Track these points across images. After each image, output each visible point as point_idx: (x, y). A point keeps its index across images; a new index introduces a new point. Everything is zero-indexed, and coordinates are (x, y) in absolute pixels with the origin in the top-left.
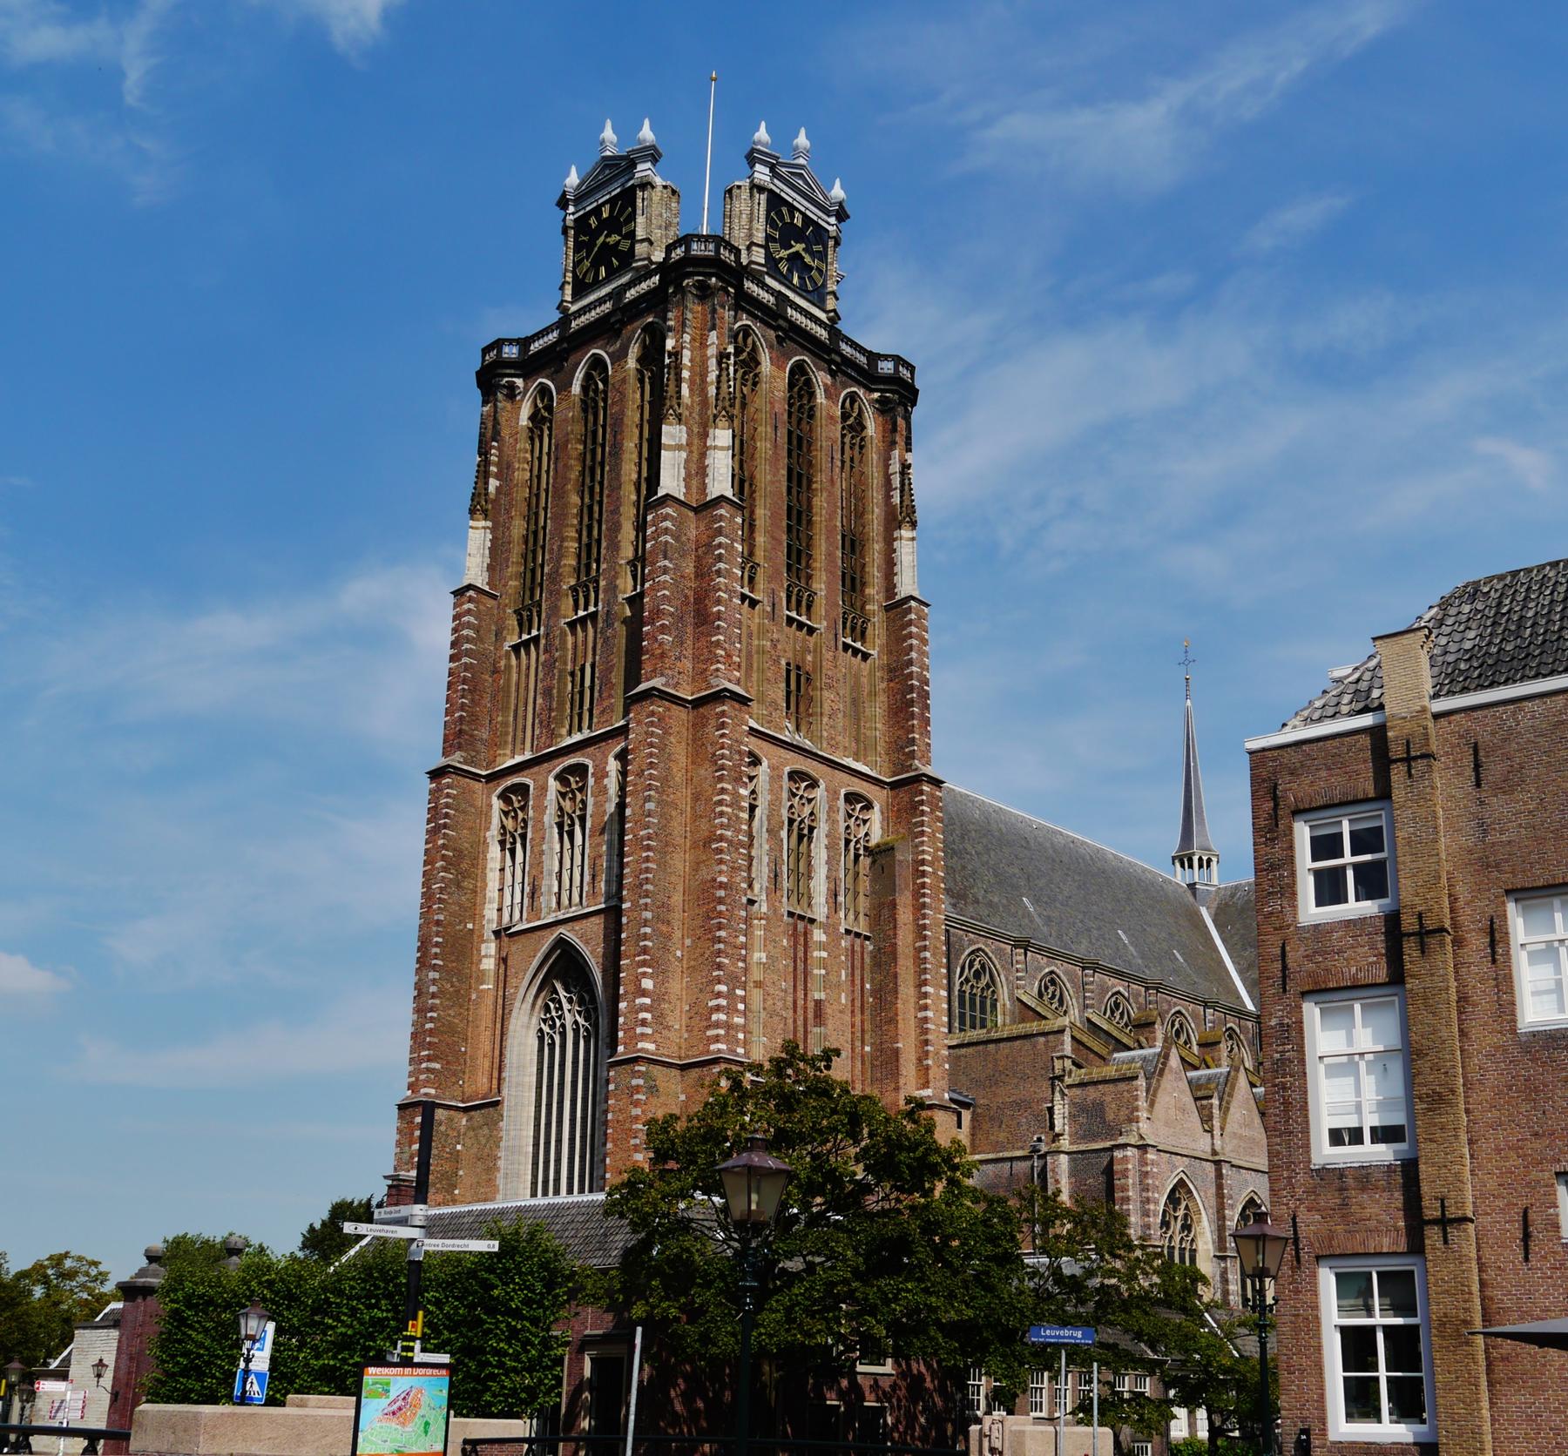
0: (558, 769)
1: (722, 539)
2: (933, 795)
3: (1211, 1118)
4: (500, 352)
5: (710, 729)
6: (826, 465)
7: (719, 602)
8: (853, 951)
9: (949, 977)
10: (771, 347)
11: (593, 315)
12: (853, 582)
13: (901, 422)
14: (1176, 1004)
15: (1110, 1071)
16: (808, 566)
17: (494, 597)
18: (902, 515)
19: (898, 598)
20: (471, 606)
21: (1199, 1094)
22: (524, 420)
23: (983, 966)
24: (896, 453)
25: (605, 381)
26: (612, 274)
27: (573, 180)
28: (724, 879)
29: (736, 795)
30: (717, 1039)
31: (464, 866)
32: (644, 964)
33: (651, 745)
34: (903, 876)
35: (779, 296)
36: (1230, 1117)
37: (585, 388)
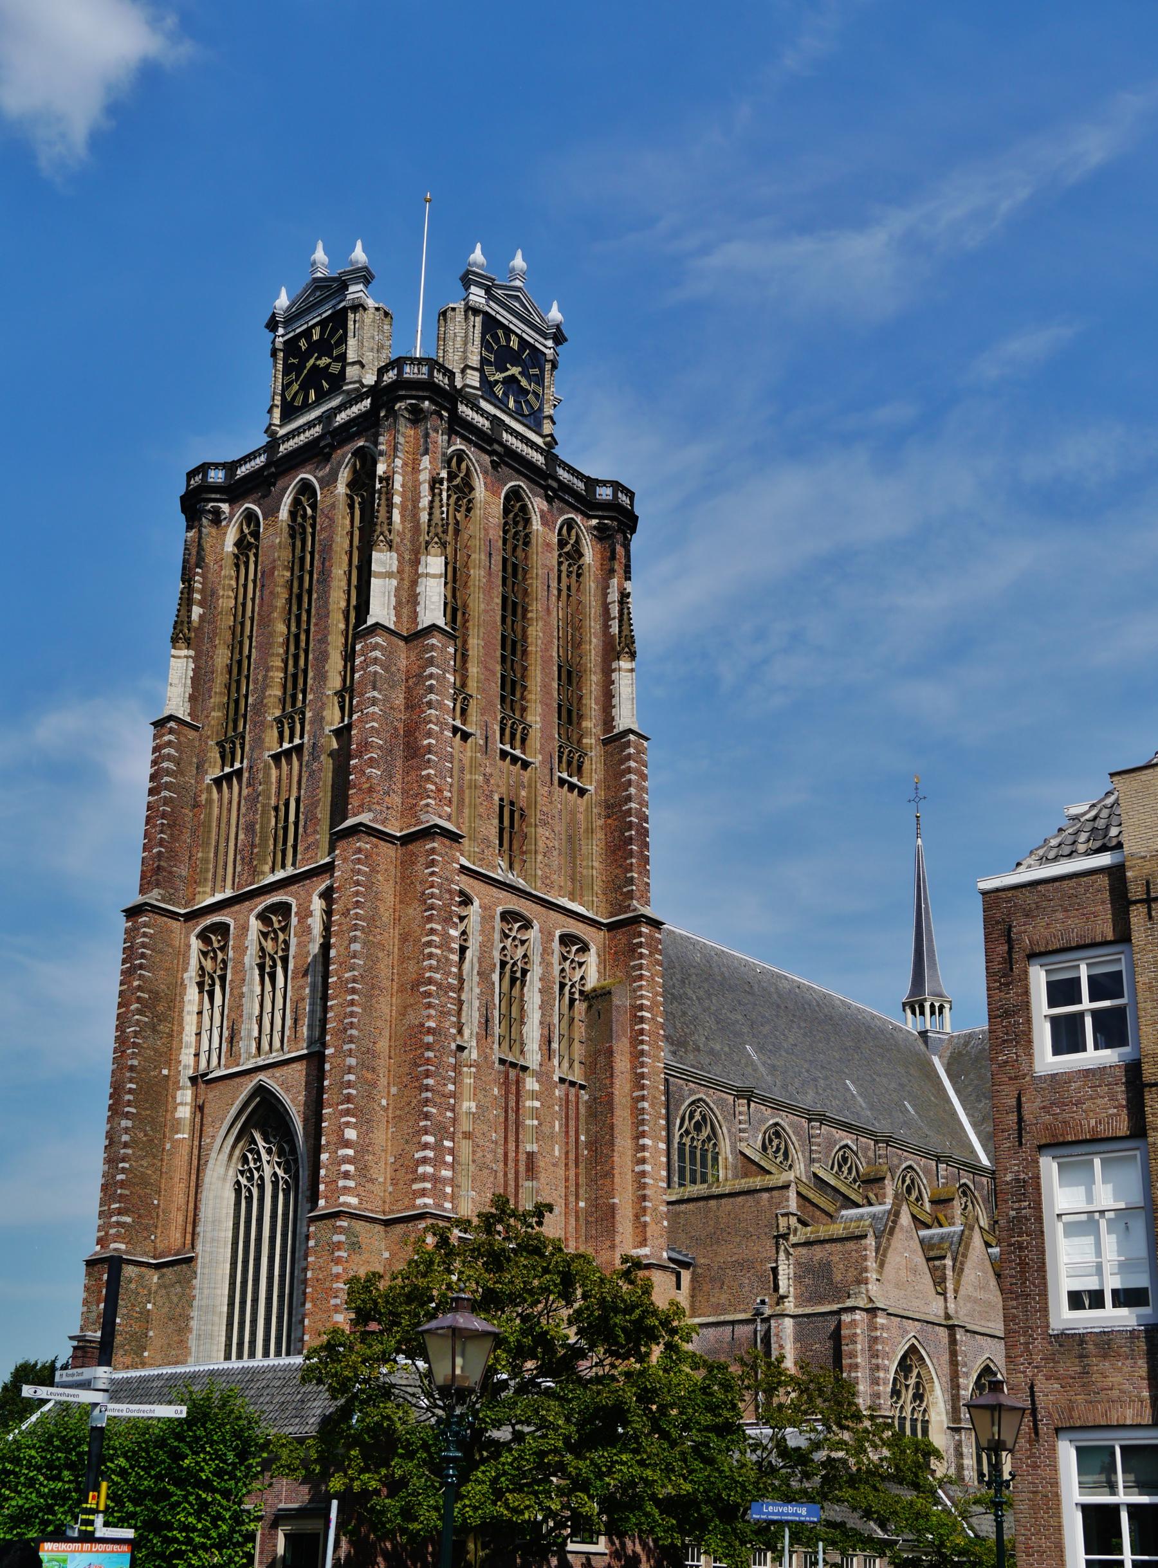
0: (260, 908)
1: (434, 670)
2: (652, 937)
3: (944, 1279)
4: (205, 476)
5: (419, 867)
6: (542, 594)
7: (429, 734)
8: (567, 1101)
9: (668, 1128)
10: (485, 472)
11: (302, 439)
12: (569, 715)
13: (619, 549)
14: (906, 1159)
15: (837, 1229)
16: (523, 698)
17: (196, 728)
18: (620, 645)
19: (616, 731)
20: (172, 737)
21: (932, 1254)
22: (229, 546)
23: (704, 1117)
24: (615, 582)
25: (314, 507)
26: (322, 397)
27: (283, 301)
28: (433, 1025)
29: (446, 937)
30: (423, 1193)
31: (160, 1008)
32: (347, 1112)
33: (358, 883)
34: (621, 1022)
35: (494, 419)
36: (964, 1280)
37: (293, 514)
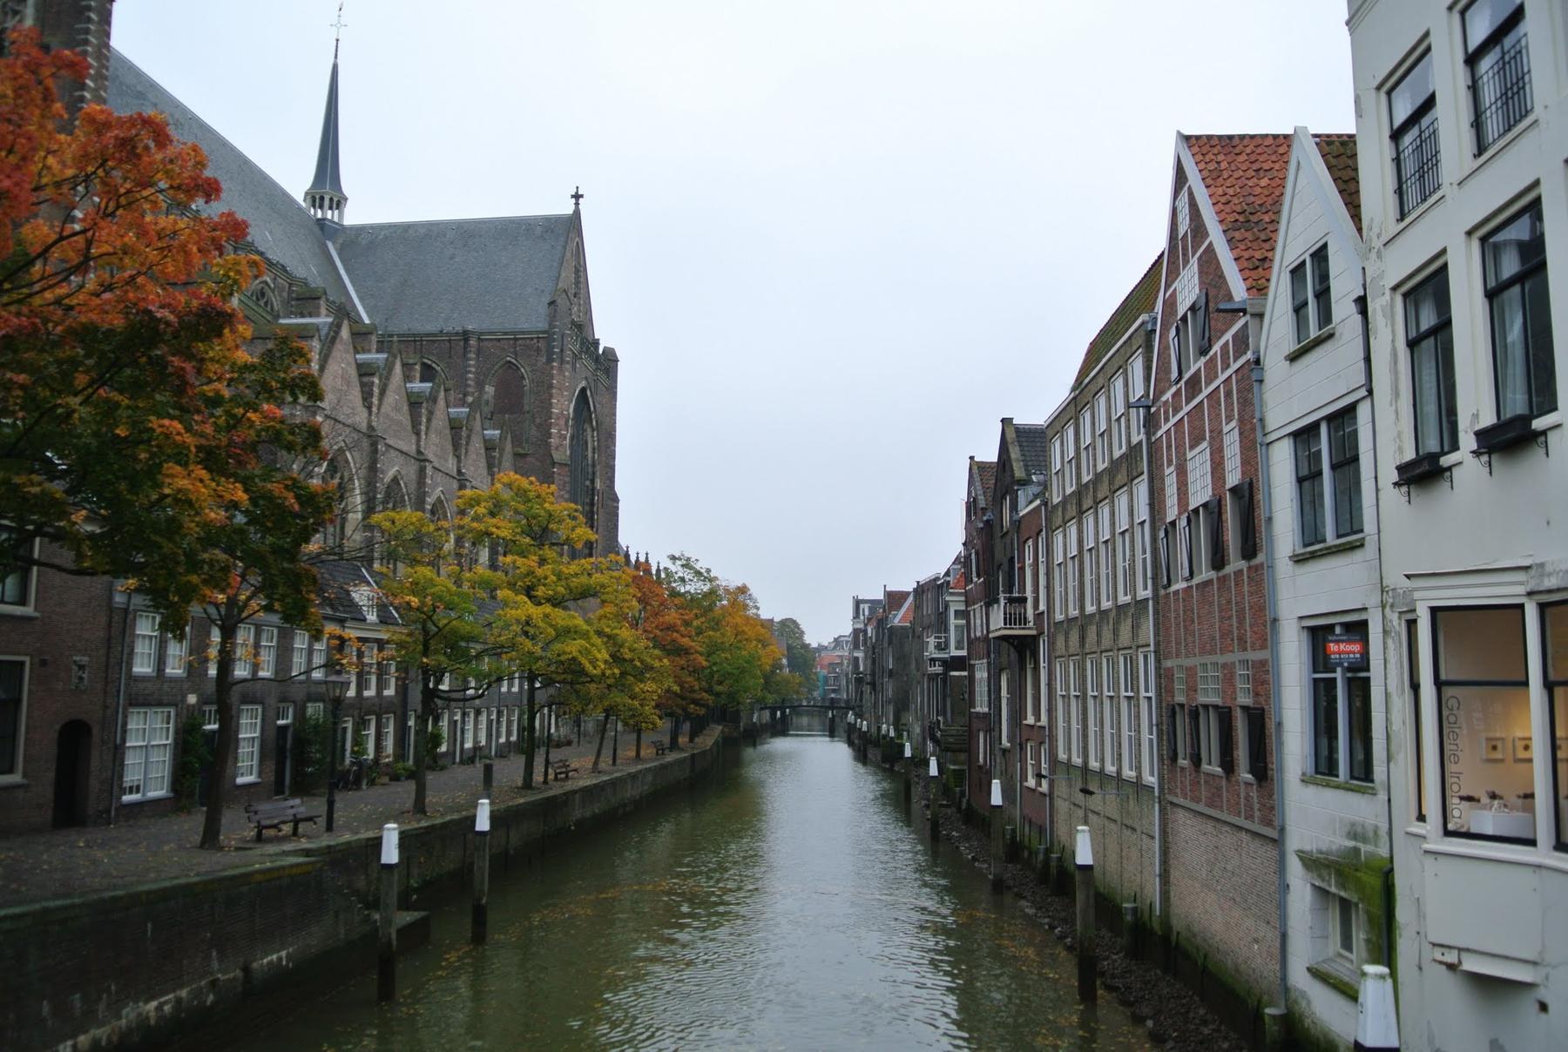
3: (371, 394)
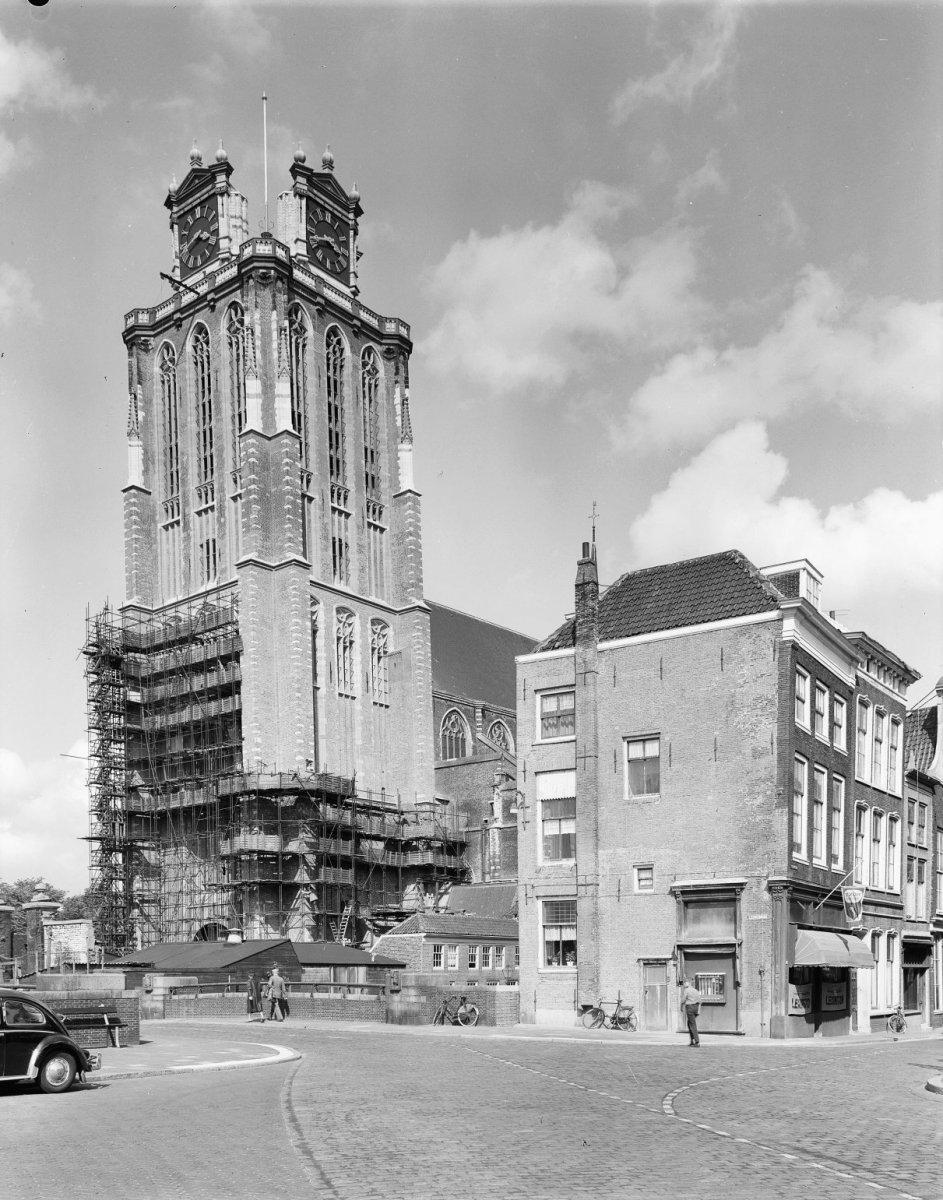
4: (137, 318)
